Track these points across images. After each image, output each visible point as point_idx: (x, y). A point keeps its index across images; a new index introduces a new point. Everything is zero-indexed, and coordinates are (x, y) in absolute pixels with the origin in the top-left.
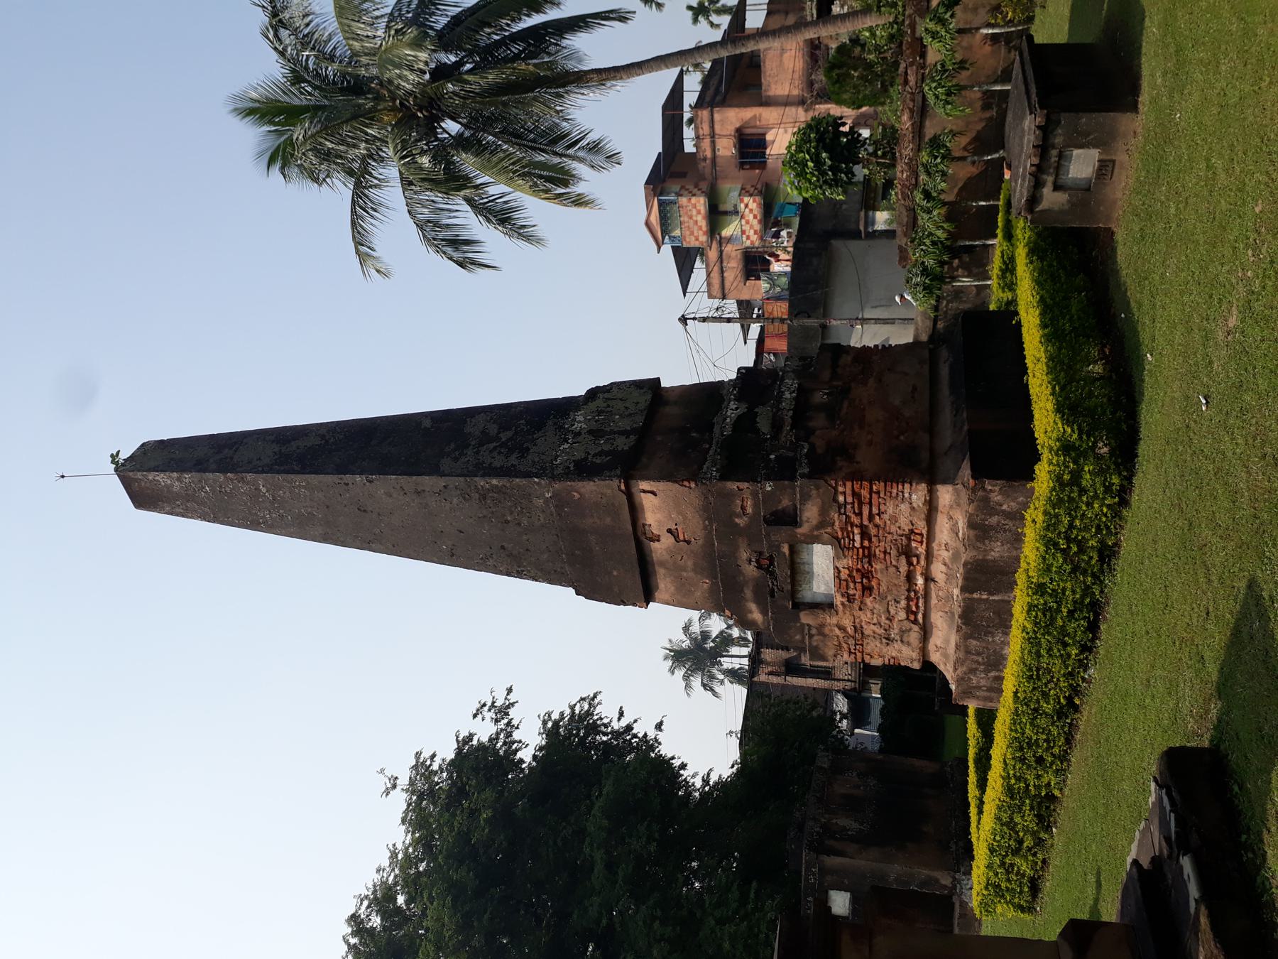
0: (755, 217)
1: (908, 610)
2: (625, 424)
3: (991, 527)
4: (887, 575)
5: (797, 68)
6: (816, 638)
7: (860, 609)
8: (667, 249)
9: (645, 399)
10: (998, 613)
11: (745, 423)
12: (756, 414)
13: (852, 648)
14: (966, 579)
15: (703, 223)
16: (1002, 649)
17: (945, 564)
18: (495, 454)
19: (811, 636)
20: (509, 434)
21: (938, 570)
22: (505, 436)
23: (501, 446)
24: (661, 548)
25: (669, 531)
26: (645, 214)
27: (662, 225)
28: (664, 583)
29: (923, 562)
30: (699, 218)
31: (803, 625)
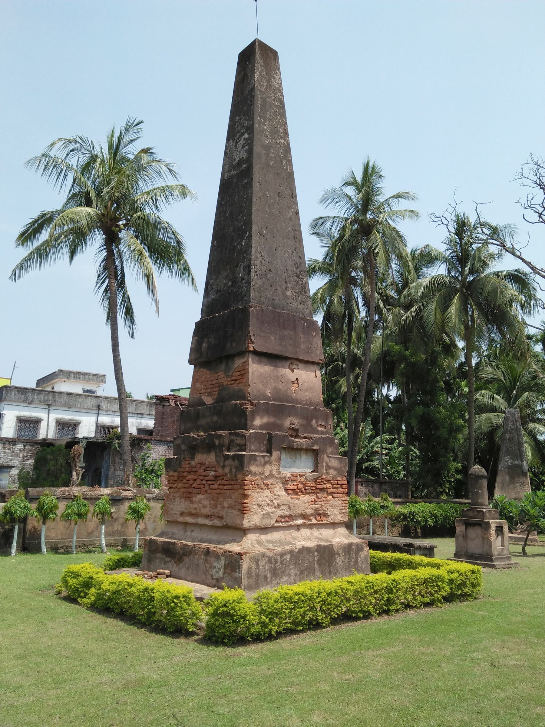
1: (281, 517)
3: (350, 555)
4: (304, 503)
6: (262, 459)
7: (280, 488)
10: (308, 568)
14: (325, 547)
16: (286, 576)
24: (286, 373)
25: (297, 379)
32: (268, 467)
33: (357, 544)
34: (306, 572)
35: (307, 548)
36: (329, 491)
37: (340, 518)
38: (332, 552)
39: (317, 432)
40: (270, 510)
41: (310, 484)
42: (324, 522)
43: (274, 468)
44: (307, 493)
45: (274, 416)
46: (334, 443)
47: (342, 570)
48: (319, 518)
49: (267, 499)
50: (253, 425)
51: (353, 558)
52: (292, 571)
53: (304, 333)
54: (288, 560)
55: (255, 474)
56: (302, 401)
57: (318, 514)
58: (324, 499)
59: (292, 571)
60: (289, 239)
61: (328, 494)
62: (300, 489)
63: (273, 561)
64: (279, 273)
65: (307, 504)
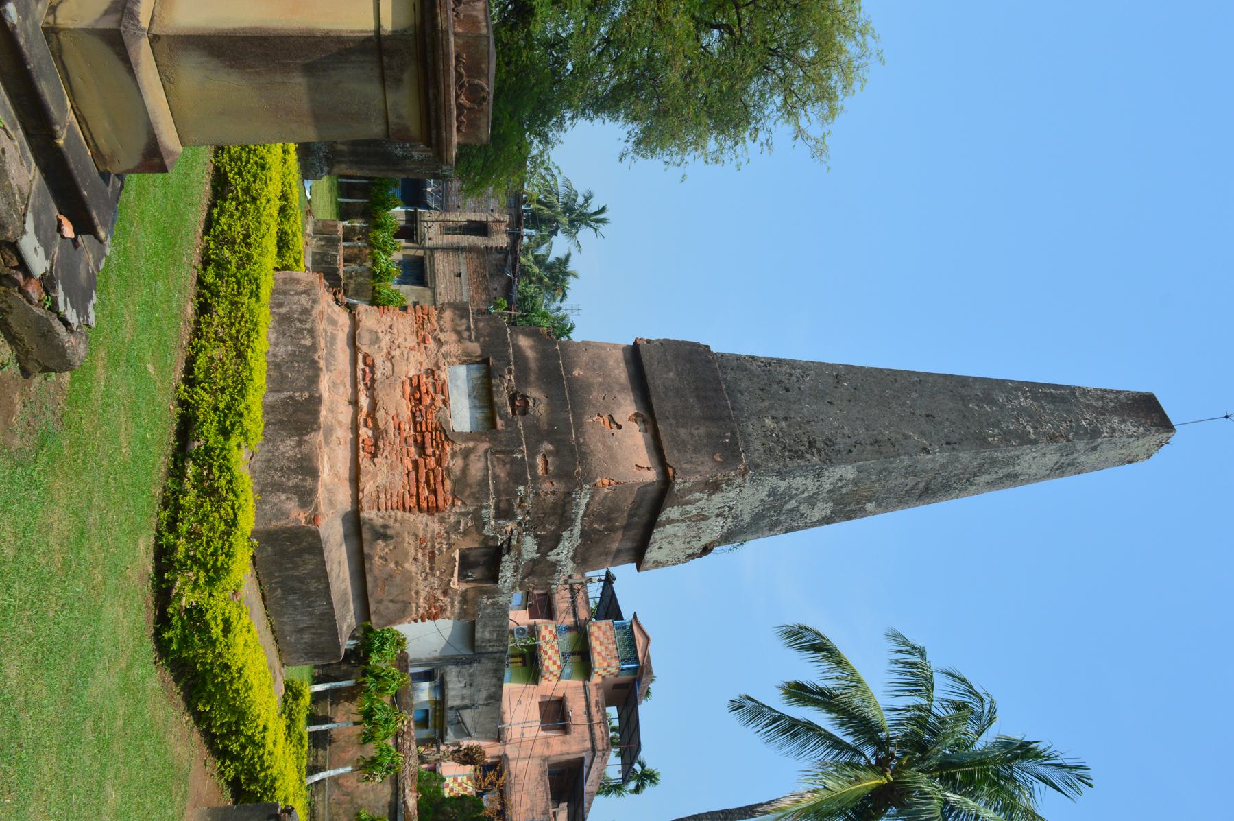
0: (546, 653)
1: (372, 367)
2: (669, 529)
3: (295, 471)
4: (396, 406)
5: (518, 794)
6: (464, 327)
7: (421, 364)
8: (627, 616)
9: (652, 554)
10: (284, 377)
11: (549, 542)
12: (538, 551)
13: (426, 321)
14: (315, 414)
15: (594, 643)
16: (277, 338)
17: (339, 422)
18: (802, 488)
19: (468, 329)
20: (788, 507)
21: (345, 414)
22: (793, 503)
23: (796, 495)
24: (627, 407)
25: (619, 427)
26: (650, 649)
27: (633, 639)
28: (620, 371)
29: (361, 421)
30: (598, 648)
31: (477, 339)
32: (454, 337)
33: (313, 492)
34: (278, 374)
35: (318, 376)
36: (421, 461)
37: (368, 486)
38: (306, 429)
39: (532, 456)
40: (385, 342)
41: (432, 422)
42: (362, 453)
43: (452, 347)
44: (413, 414)
45: (540, 369)
46: (517, 483)
47: (269, 451)
48: (369, 443)
49: (400, 340)
50: (517, 334)
51: (288, 479)
52: (283, 349)
53: (709, 436)
54: (302, 342)
55: (440, 318)
56: (583, 434)
57: (378, 434)
58: (405, 451)
59: (283, 349)
60: (867, 430)
61: (415, 463)
62: (420, 401)
63: (303, 317)
64: (795, 407)
65: (393, 412)
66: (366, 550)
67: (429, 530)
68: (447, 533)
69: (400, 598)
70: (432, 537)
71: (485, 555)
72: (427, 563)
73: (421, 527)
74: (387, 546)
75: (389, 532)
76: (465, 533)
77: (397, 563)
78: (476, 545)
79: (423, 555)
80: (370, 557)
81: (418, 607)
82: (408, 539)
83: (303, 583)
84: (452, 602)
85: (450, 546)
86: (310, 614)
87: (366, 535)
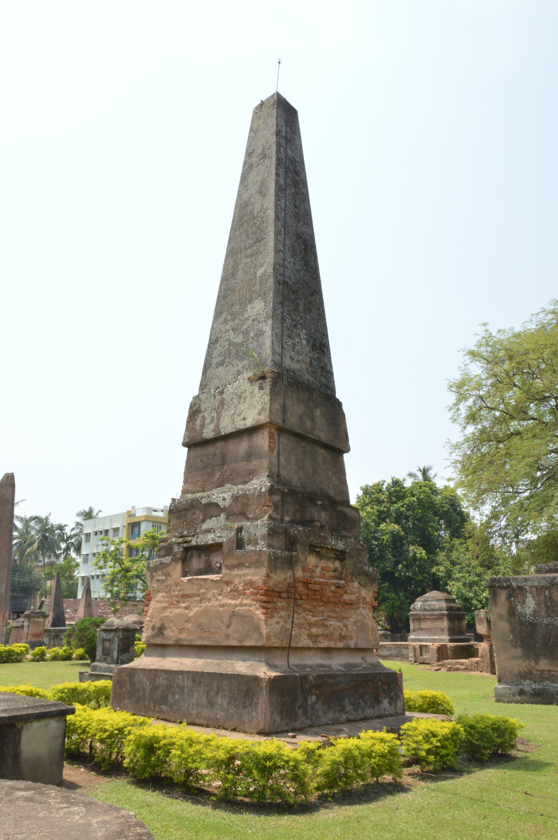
66: (170, 642)
67: (161, 599)
68: (167, 587)
69: (226, 618)
70: (168, 597)
71: (199, 556)
72: (192, 600)
73: (159, 605)
74: (170, 628)
75: (158, 626)
76: (167, 575)
77: (188, 621)
78: (179, 566)
79: (184, 602)
80: (178, 640)
81: (241, 604)
82: (167, 613)
83: (158, 688)
84: (240, 576)
85: (177, 585)
86: (191, 690)
87: (158, 641)
